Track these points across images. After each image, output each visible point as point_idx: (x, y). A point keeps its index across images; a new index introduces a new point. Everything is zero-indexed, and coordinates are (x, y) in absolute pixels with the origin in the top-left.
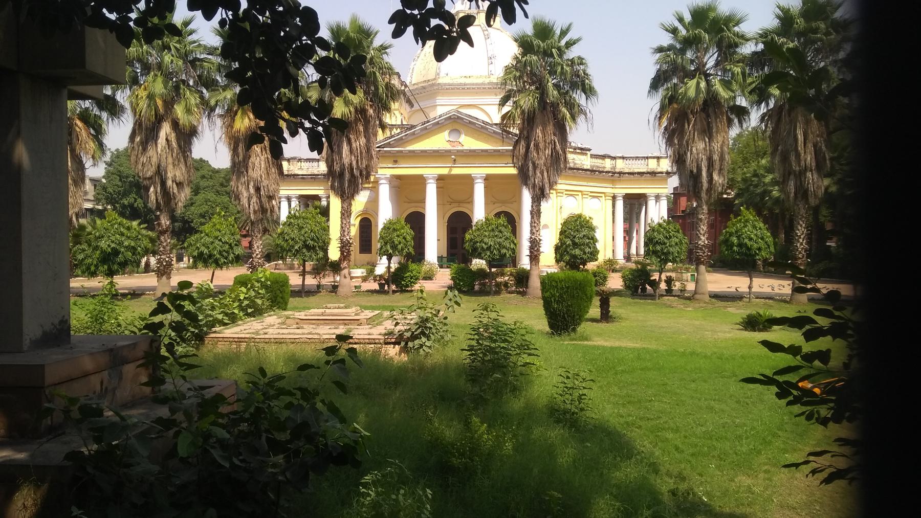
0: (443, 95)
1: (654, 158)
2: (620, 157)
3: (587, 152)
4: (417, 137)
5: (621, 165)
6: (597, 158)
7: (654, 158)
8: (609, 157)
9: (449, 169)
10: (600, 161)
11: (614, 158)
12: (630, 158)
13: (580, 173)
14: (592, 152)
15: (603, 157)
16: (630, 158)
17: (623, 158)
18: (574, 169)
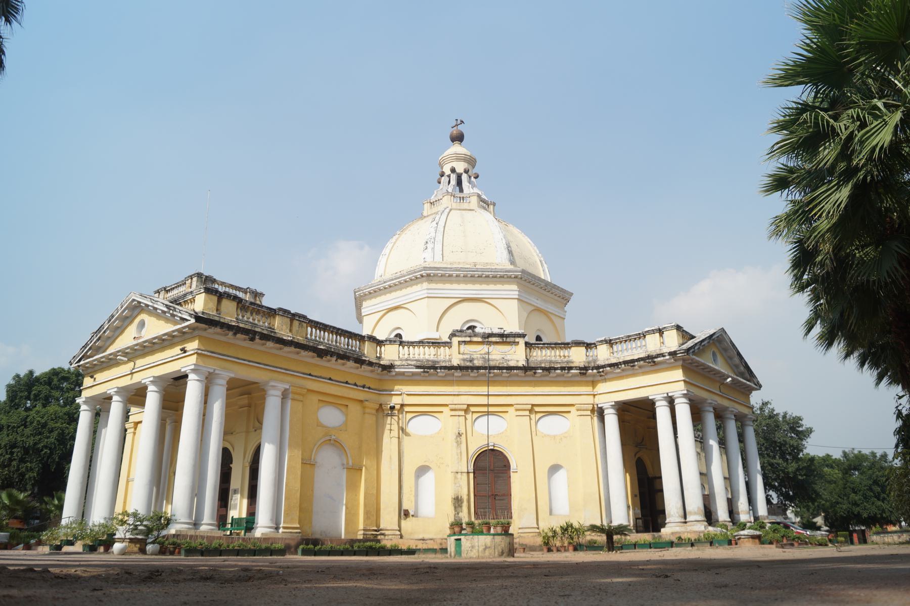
0: (365, 300)
1: (653, 332)
2: (601, 341)
3: (517, 340)
4: (112, 340)
5: (603, 355)
6: (553, 348)
7: (653, 332)
8: (578, 344)
9: (130, 376)
10: (565, 352)
11: (589, 346)
12: (621, 341)
13: (496, 375)
14: (527, 339)
15: (566, 345)
16: (621, 341)
17: (610, 343)
18: (478, 368)
